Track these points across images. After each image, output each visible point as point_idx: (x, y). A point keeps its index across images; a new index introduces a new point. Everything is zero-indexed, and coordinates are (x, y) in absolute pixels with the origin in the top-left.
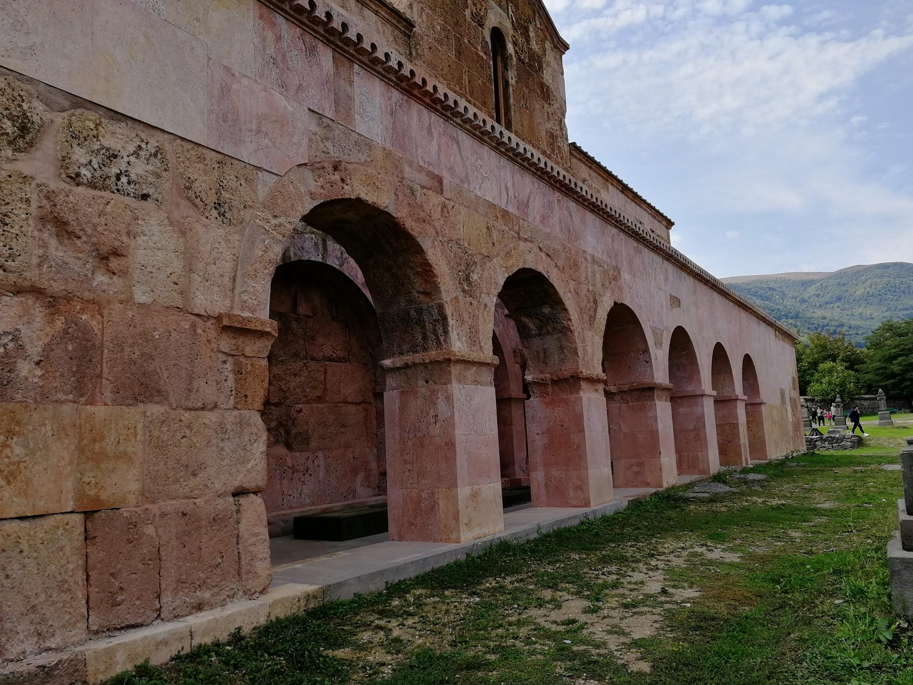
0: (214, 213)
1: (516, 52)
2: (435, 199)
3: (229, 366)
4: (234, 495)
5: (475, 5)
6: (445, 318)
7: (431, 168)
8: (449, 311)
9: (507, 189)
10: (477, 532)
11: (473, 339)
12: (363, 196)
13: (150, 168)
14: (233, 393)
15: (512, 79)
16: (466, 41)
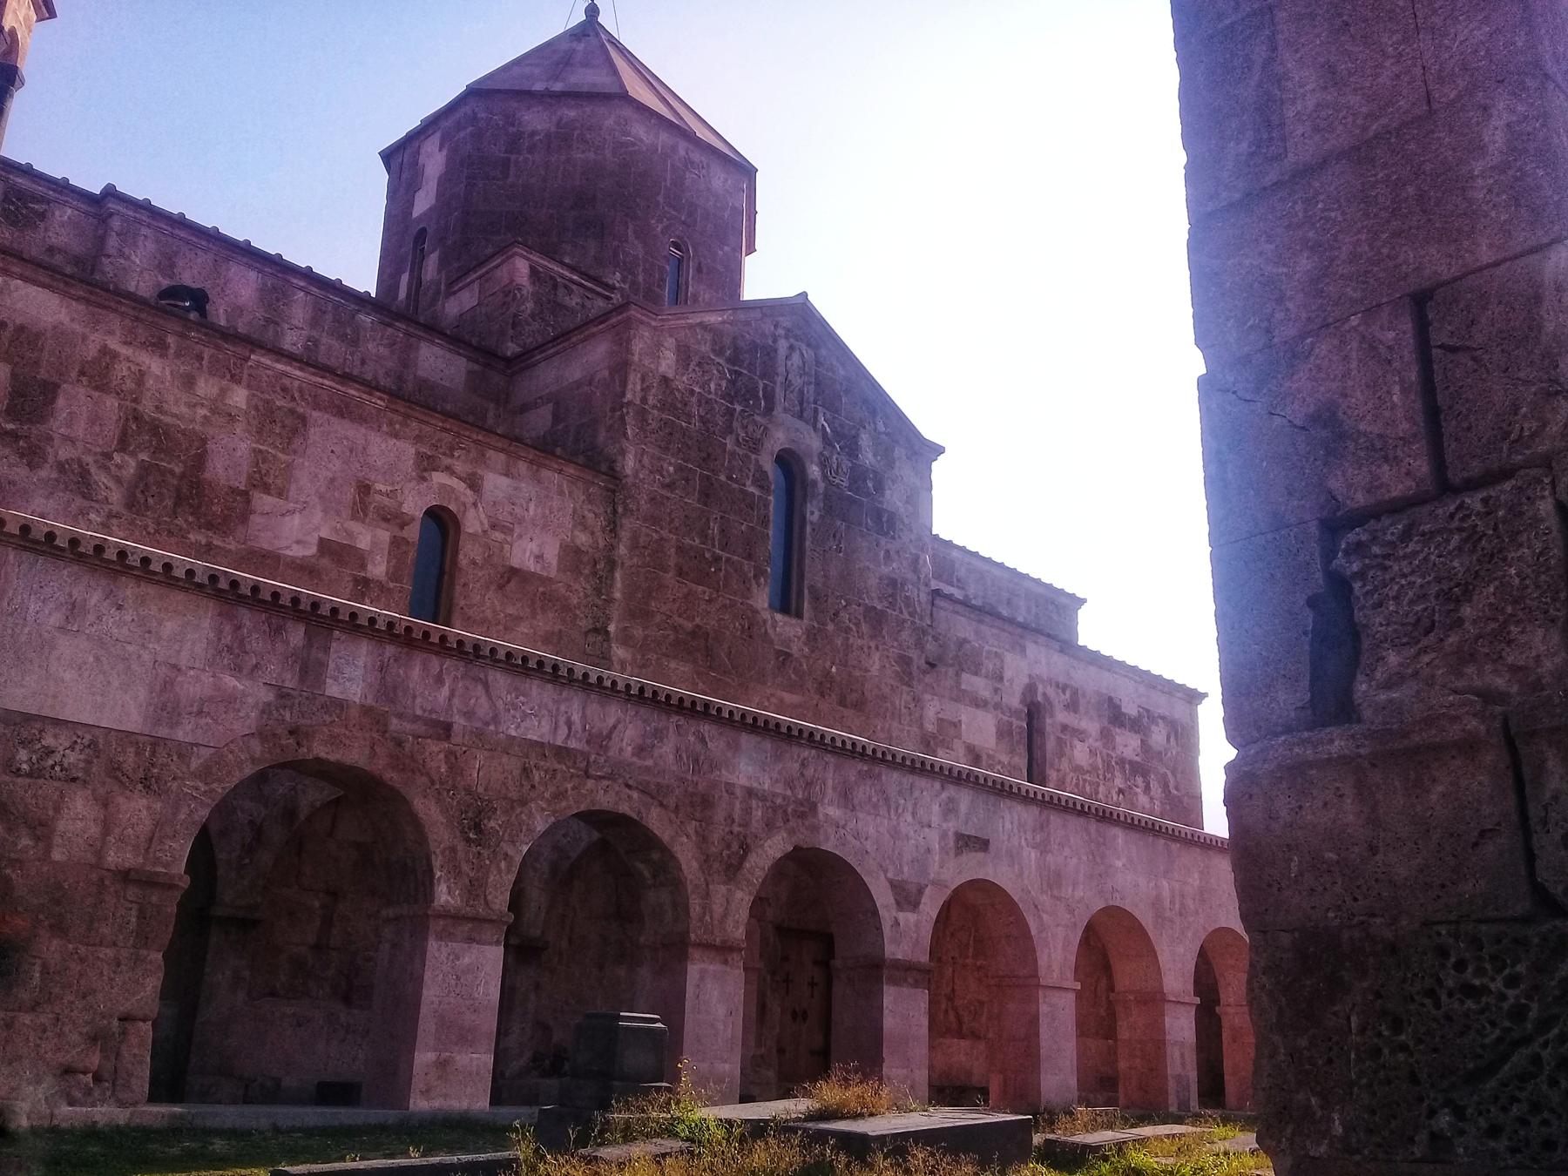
0: (140, 787)
1: (825, 477)
2: (433, 747)
3: (134, 913)
4: (120, 1020)
5: (745, 427)
6: (431, 870)
7: (434, 716)
8: (437, 862)
9: (569, 724)
10: (437, 1103)
11: (475, 889)
12: (323, 755)
13: (82, 757)
14: (134, 934)
15: (812, 513)
16: (723, 478)
